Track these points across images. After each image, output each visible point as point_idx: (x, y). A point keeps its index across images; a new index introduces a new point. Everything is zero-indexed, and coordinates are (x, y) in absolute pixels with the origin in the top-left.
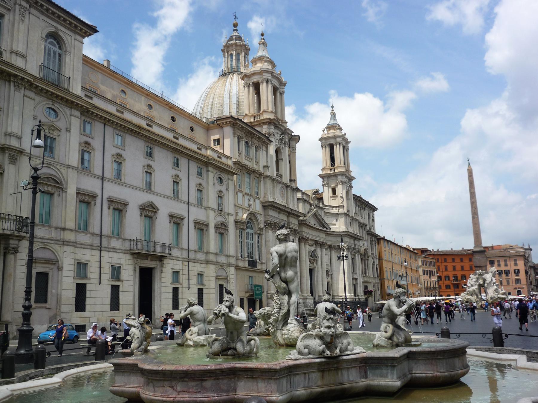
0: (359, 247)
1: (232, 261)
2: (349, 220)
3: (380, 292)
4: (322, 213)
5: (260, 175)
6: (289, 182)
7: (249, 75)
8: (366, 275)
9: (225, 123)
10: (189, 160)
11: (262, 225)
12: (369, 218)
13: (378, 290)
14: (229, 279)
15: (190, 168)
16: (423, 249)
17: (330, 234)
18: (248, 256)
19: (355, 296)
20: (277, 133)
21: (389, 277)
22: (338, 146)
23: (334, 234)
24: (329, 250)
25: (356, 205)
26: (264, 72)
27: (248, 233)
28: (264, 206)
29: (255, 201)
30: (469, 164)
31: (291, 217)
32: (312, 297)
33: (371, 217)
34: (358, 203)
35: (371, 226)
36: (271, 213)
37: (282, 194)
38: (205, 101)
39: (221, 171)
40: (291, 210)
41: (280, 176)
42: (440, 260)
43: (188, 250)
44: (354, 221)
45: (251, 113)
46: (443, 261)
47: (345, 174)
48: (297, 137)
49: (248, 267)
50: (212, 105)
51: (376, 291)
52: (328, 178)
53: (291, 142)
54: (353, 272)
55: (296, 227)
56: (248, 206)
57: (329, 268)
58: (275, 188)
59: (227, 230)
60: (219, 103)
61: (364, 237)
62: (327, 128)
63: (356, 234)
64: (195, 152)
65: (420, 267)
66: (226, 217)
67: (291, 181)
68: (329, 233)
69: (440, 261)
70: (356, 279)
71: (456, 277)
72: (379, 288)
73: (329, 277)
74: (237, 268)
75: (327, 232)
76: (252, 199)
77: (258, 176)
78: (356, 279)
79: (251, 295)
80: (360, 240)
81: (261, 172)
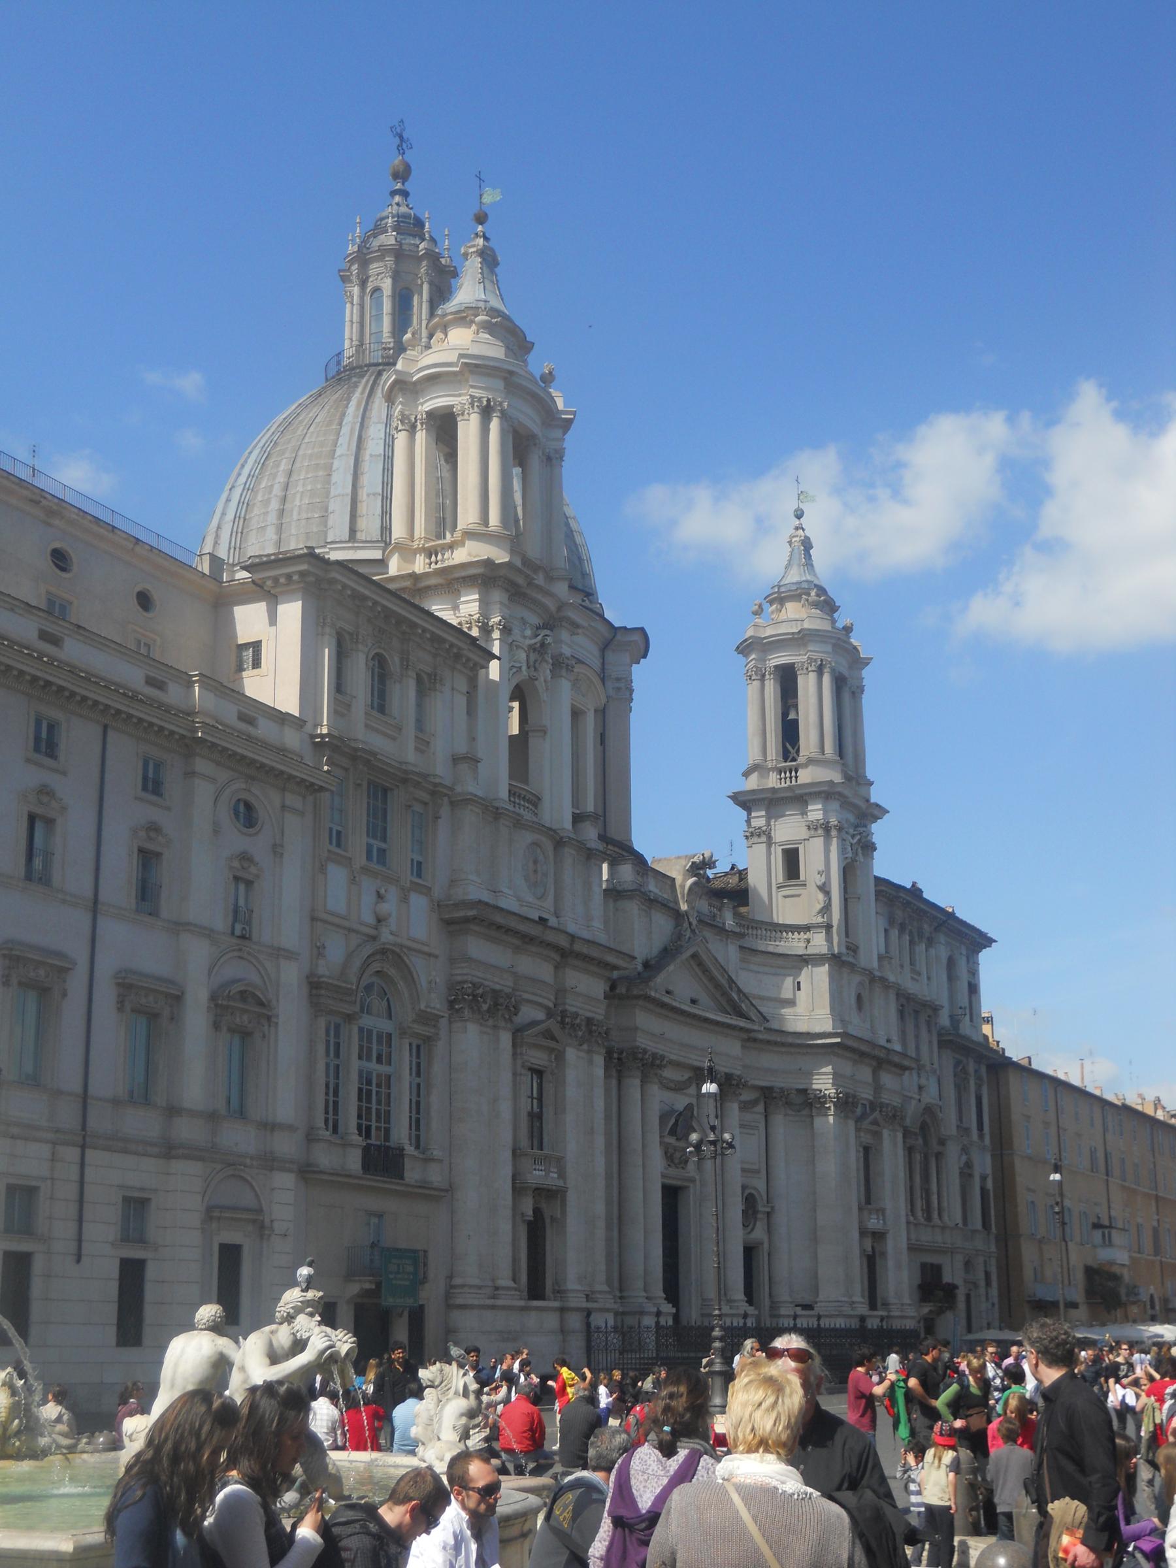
0: (896, 1101)
1: (287, 1146)
3: (994, 1292)
5: (437, 792)
6: (568, 824)
8: (929, 1218)
9: (282, 580)
10: (105, 727)
11: (436, 1003)
12: (952, 978)
13: (988, 1283)
14: (267, 1222)
15: (108, 763)
18: (360, 1129)
19: (873, 1306)
20: (523, 621)
22: (812, 676)
23: (783, 1044)
24: (760, 1108)
25: (891, 921)
27: (370, 1032)
28: (449, 923)
29: (405, 899)
32: (668, 1308)
33: (964, 977)
34: (899, 914)
35: (960, 1011)
36: (478, 948)
37: (535, 871)
38: (259, 480)
40: (573, 938)
41: (534, 798)
43: (85, 1096)
45: (417, 535)
47: (840, 794)
48: (636, 637)
50: (284, 499)
51: (976, 1285)
53: (610, 656)
54: (868, 1201)
55: (598, 1012)
56: (371, 920)
57: (761, 1185)
59: (269, 1018)
61: (925, 1059)
63: (883, 1042)
64: (133, 697)
68: (760, 1036)
70: (878, 1236)
72: (994, 1277)
73: (758, 1224)
74: (307, 1172)
75: (752, 1035)
76: (393, 894)
77: (425, 796)
78: (878, 1236)
79: (367, 1293)
80: (904, 1068)
81: (437, 780)
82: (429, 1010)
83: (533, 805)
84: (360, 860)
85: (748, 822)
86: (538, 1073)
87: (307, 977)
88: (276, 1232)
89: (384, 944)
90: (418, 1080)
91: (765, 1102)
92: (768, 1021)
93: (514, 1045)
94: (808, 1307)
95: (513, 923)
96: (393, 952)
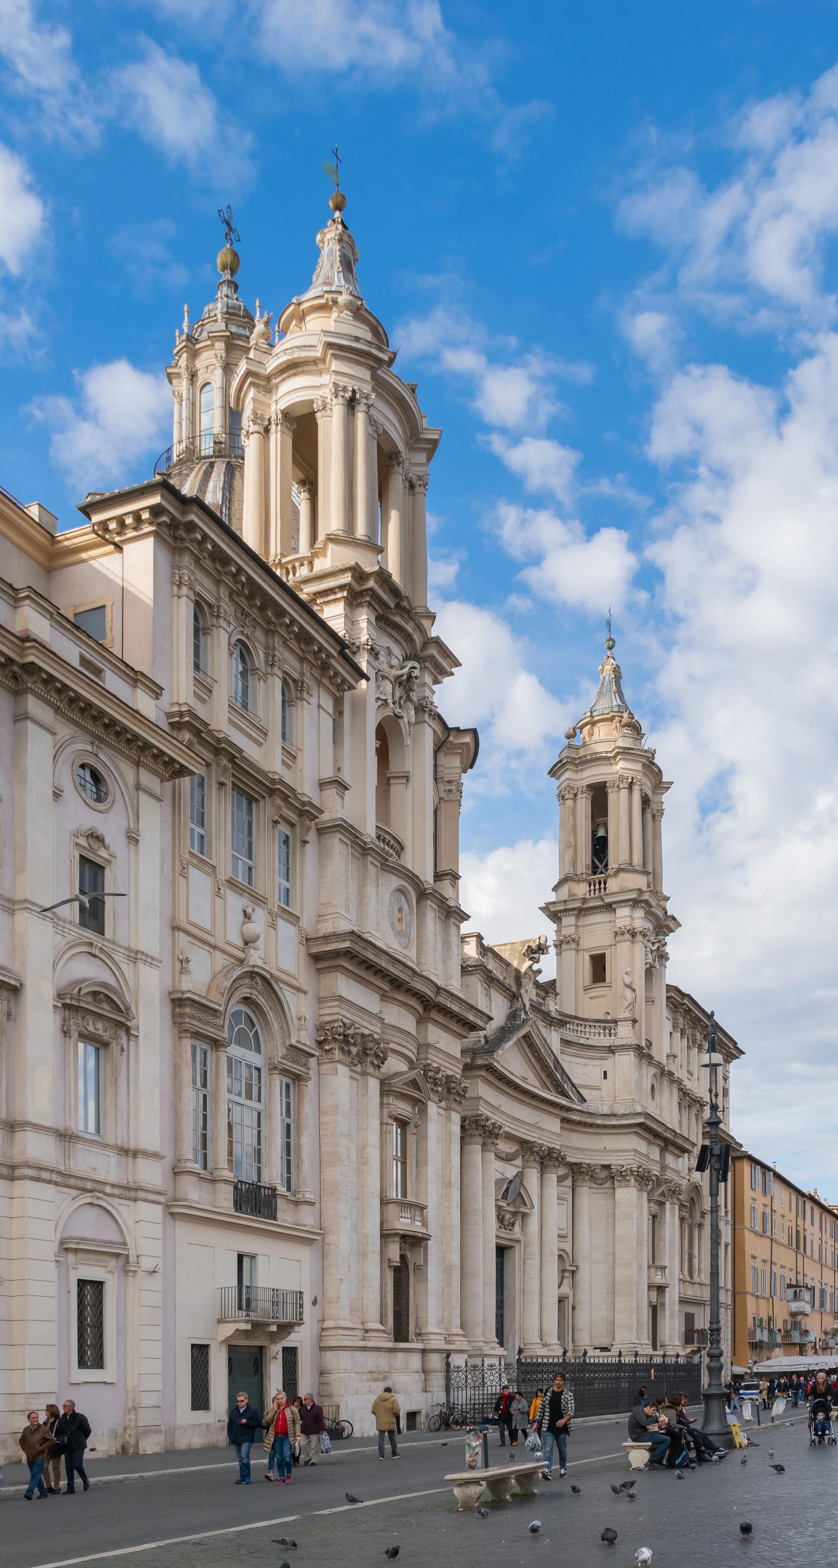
2: (650, 1076)
4: (554, 1038)
17: (579, 1123)
23: (591, 1125)
24: (569, 1182)
28: (316, 958)
29: (273, 926)
31: (436, 1023)
37: (400, 920)
40: (438, 989)
44: (666, 1083)
58: (371, 890)
59: (128, 1030)
66: (124, 968)
67: (439, 876)
70: (661, 1289)
78: (661, 1289)
82: (300, 1046)
83: (396, 853)
84: (225, 871)
87: (169, 993)
88: (143, 1268)
89: (254, 966)
90: (287, 1120)
91: (573, 1177)
92: (585, 1101)
95: (384, 964)
96: (263, 978)
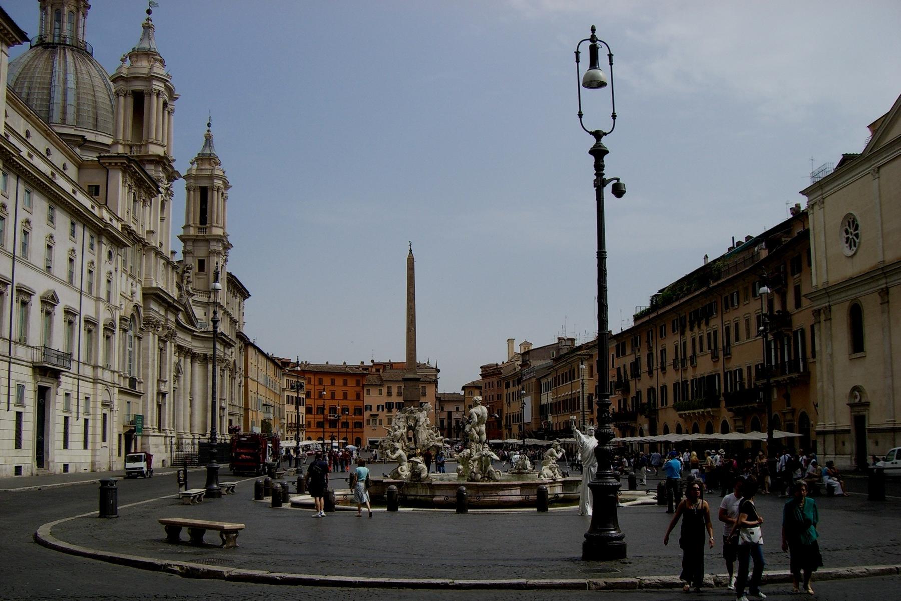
7: (127, 78)
16: (284, 360)
21: (253, 409)
26: (155, 79)
30: (411, 251)
36: (153, 306)
39: (112, 242)
42: (312, 380)
46: (317, 383)
49: (128, 388)
52: (193, 242)
56: (130, 295)
60: (42, 99)
62: (197, 159)
65: (284, 390)
69: (312, 383)
71: (333, 410)
85: (185, 247)
86: (161, 350)
93: (159, 340)
94: (203, 435)
